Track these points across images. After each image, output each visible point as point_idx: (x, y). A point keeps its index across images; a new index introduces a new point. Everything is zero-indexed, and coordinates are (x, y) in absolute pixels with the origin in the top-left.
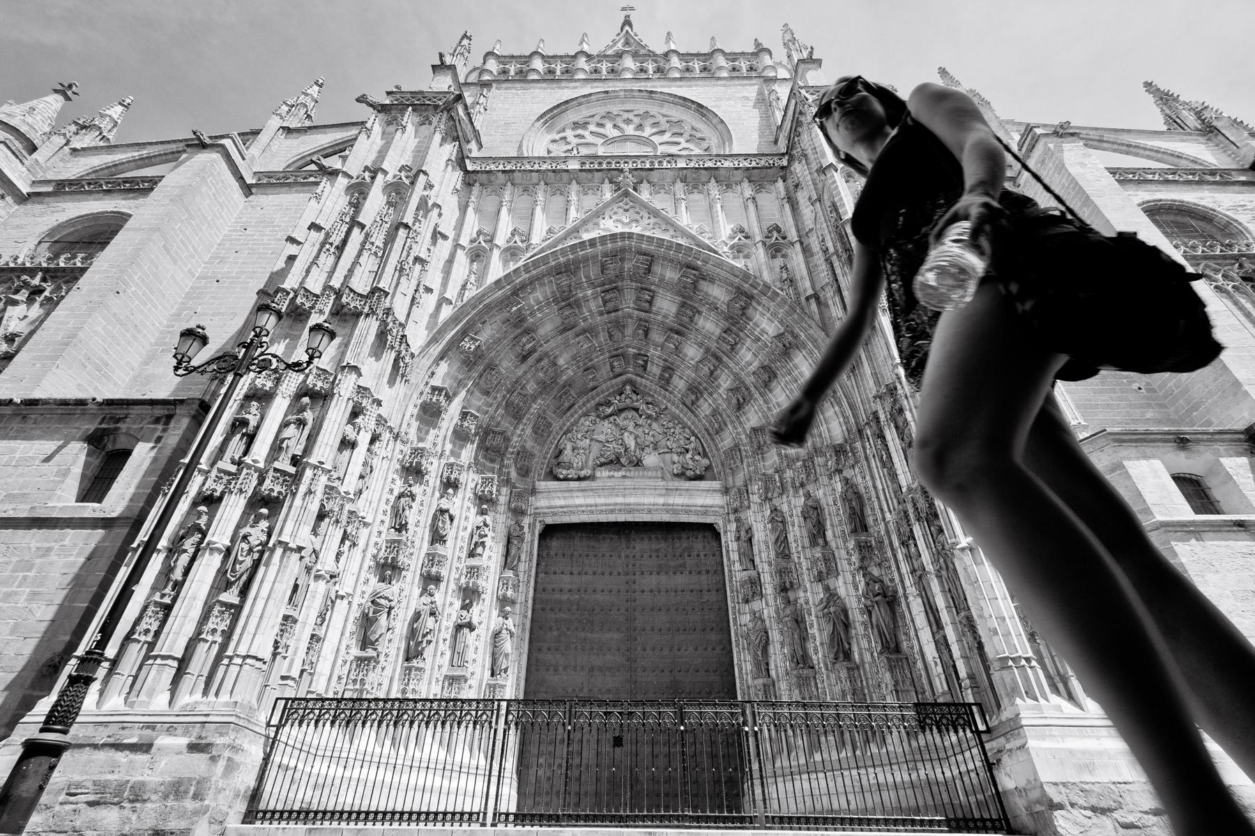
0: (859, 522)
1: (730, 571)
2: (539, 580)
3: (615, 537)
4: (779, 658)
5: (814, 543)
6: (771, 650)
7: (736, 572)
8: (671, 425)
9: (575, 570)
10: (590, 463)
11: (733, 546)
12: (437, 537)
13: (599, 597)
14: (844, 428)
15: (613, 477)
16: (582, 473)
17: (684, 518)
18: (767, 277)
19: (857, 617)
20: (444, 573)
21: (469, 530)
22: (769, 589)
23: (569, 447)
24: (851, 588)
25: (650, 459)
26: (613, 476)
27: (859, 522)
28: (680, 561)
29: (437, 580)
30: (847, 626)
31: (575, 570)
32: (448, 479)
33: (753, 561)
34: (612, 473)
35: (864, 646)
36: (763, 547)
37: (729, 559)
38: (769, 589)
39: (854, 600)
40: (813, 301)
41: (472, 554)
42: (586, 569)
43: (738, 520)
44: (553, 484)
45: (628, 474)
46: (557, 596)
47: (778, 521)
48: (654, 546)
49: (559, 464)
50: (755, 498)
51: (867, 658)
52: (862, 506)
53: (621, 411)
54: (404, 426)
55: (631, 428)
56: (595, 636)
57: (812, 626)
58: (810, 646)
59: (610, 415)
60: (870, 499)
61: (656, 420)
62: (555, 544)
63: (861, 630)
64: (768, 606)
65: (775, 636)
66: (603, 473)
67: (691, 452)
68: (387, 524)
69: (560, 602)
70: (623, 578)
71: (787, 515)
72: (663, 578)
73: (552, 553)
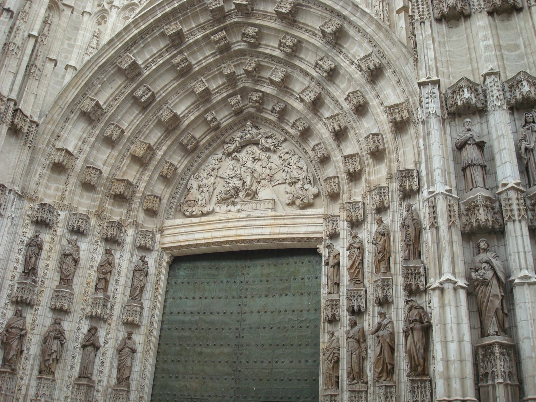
2: (168, 304)
8: (288, 156)
9: (197, 295)
15: (230, 211)
25: (265, 193)
26: (230, 211)
34: (229, 208)
45: (243, 208)
48: (266, 271)
61: (275, 152)
62: (182, 272)
67: (300, 183)
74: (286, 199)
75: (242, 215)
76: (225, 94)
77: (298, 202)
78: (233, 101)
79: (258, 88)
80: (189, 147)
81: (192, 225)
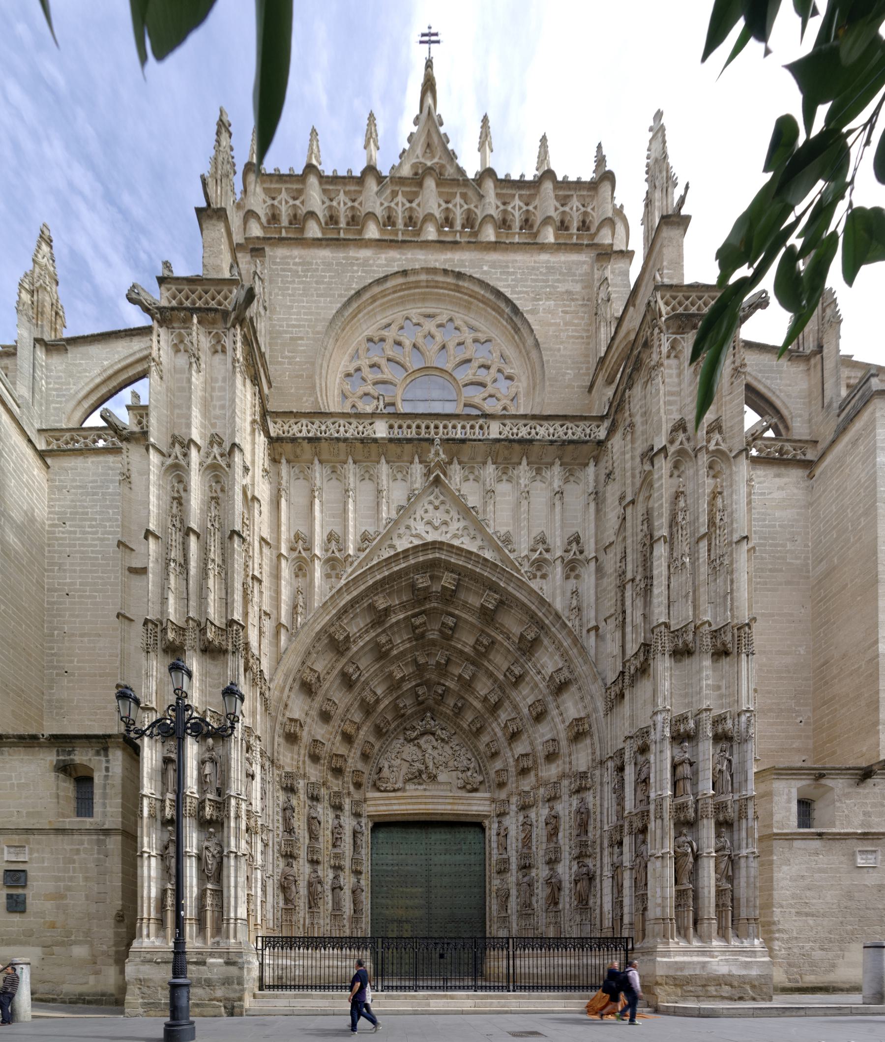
0: (583, 826)
1: (490, 853)
3: (418, 831)
4: (513, 904)
5: (549, 840)
6: (511, 899)
7: (495, 855)
9: (395, 852)
10: (401, 778)
11: (494, 838)
12: (313, 836)
13: (409, 868)
14: (590, 758)
16: (396, 786)
17: (463, 819)
18: (559, 605)
19: (567, 885)
20: (321, 858)
21: (330, 829)
22: (514, 867)
23: (386, 766)
24: (567, 868)
27: (583, 826)
28: (459, 847)
29: (317, 862)
30: (559, 889)
31: (395, 852)
32: (312, 794)
33: (506, 848)
35: (566, 900)
36: (514, 840)
37: (490, 846)
38: (514, 867)
39: (567, 876)
40: (593, 633)
41: (334, 846)
42: (401, 852)
43: (499, 822)
44: (378, 795)
46: (385, 867)
47: (527, 825)
48: (444, 837)
49: (380, 779)
50: (513, 808)
51: (567, 906)
52: (588, 816)
53: (423, 734)
54: (276, 754)
55: (430, 751)
56: (408, 890)
57: (537, 888)
58: (534, 899)
59: (416, 738)
60: (595, 813)
62: (382, 835)
63: (567, 892)
64: (513, 877)
65: (514, 892)
66: (410, 787)
68: (281, 829)
69: (387, 871)
70: (423, 857)
71: (534, 821)
72: (448, 857)
73: (380, 841)
74: (460, 783)
75: (427, 793)
76: (414, 683)
77: (469, 787)
78: (421, 691)
79: (442, 681)
80: (384, 730)
81: (389, 798)
